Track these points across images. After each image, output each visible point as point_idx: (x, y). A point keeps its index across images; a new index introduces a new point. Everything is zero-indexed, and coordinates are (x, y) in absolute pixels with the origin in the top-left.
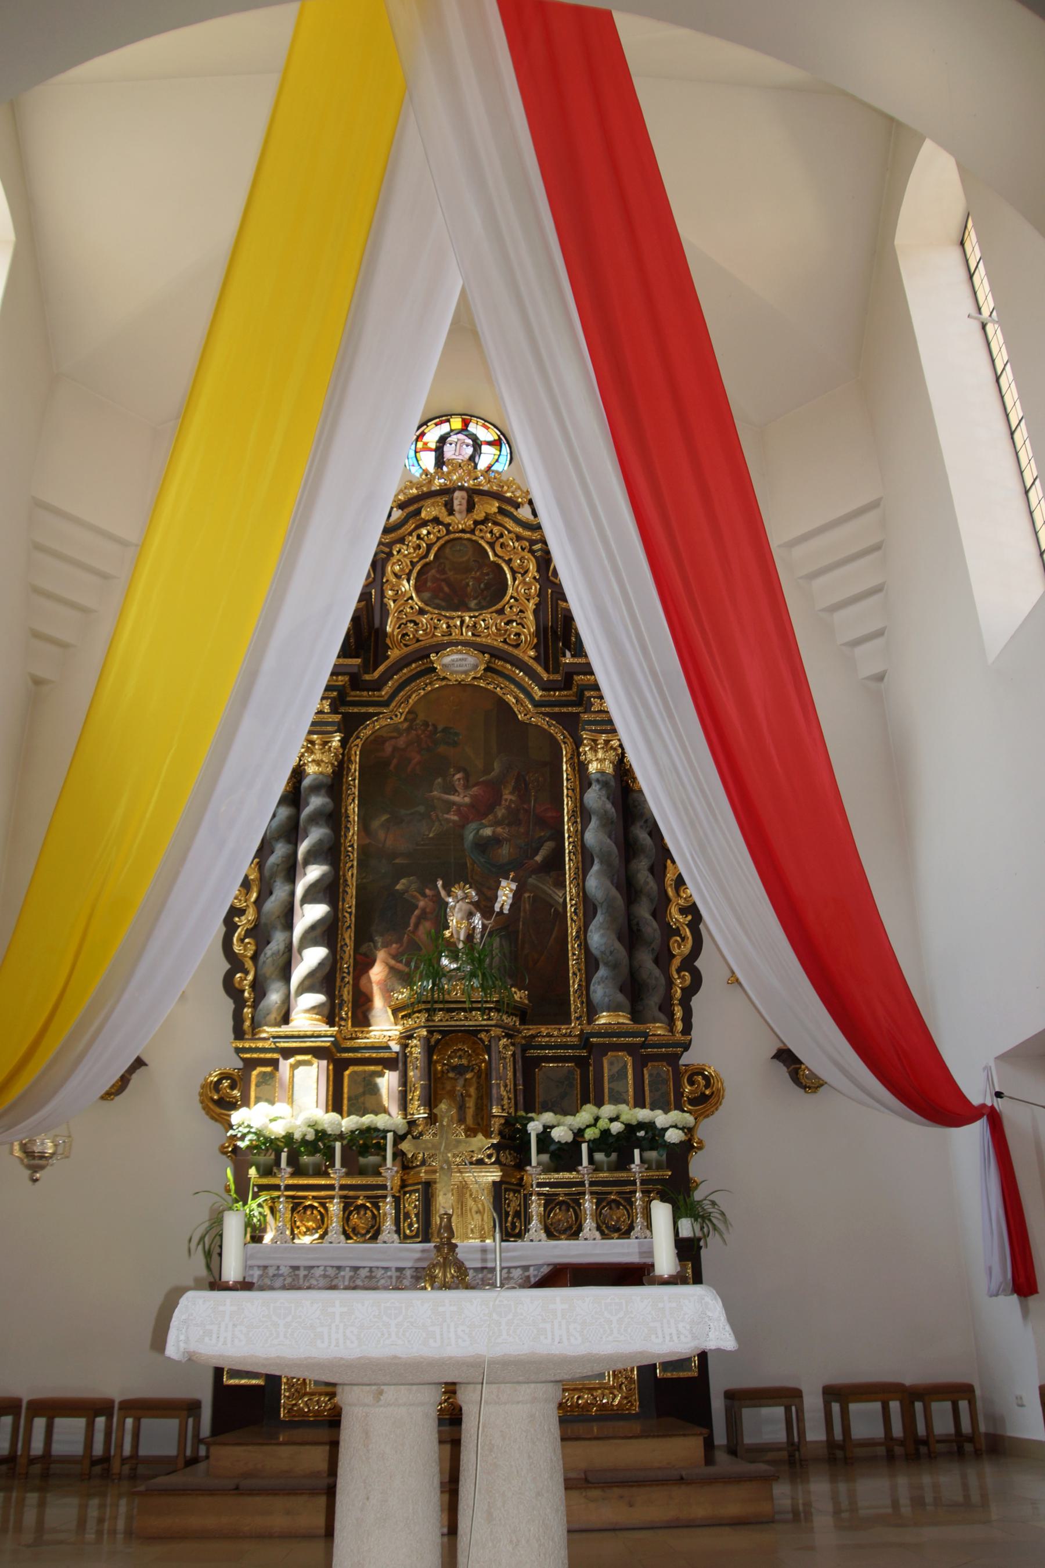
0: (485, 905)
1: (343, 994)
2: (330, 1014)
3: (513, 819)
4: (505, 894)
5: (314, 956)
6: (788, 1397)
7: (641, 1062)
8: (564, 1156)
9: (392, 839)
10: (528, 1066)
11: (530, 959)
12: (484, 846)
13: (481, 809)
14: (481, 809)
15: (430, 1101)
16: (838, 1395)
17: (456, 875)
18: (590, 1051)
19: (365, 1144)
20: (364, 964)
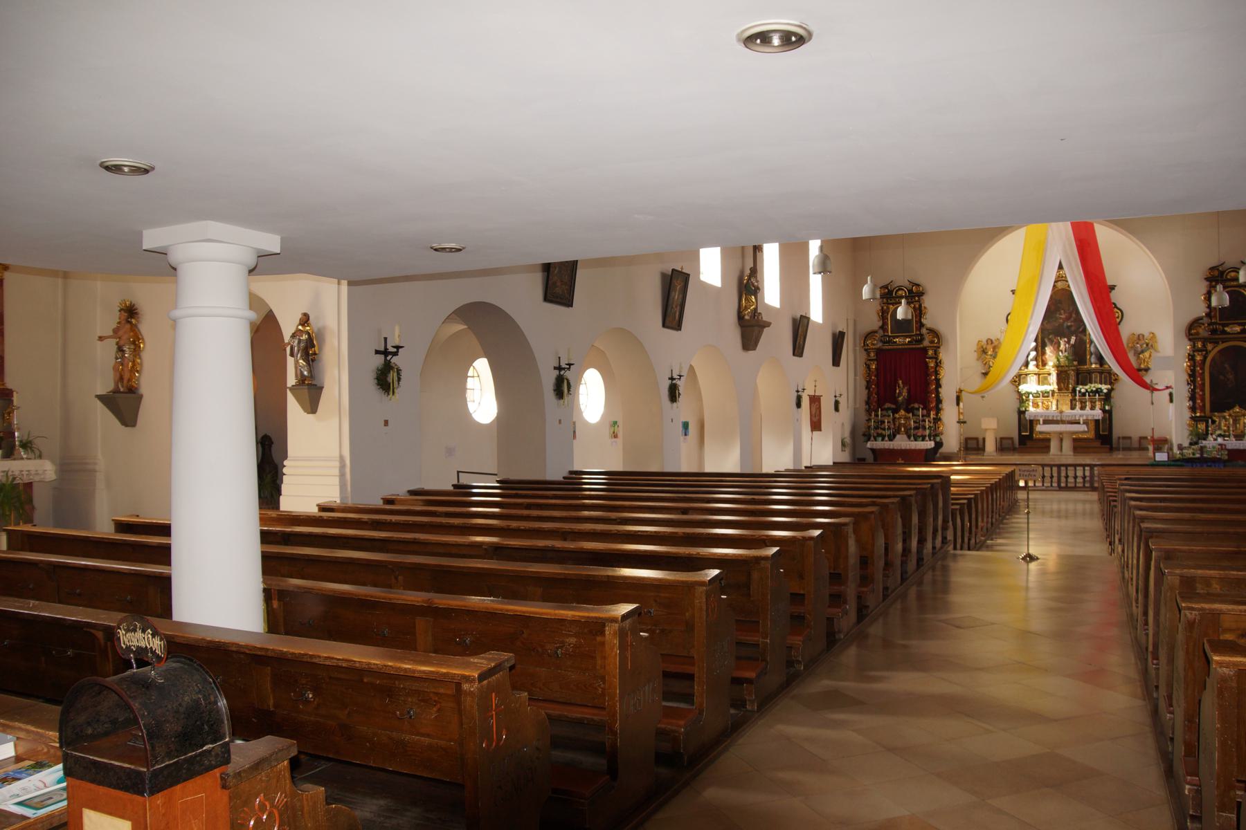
0: (1068, 342)
1: (1041, 361)
2: (1037, 366)
3: (1075, 320)
4: (1073, 340)
5: (1033, 354)
6: (1130, 438)
7: (1101, 373)
8: (1084, 395)
9: (1048, 326)
10: (1078, 373)
11: (1080, 352)
12: (1069, 327)
13: (1068, 319)
14: (1068, 319)
15: (1058, 384)
16: (1141, 438)
17: (1062, 336)
18: (1090, 372)
19: (1045, 394)
20: (1044, 353)
